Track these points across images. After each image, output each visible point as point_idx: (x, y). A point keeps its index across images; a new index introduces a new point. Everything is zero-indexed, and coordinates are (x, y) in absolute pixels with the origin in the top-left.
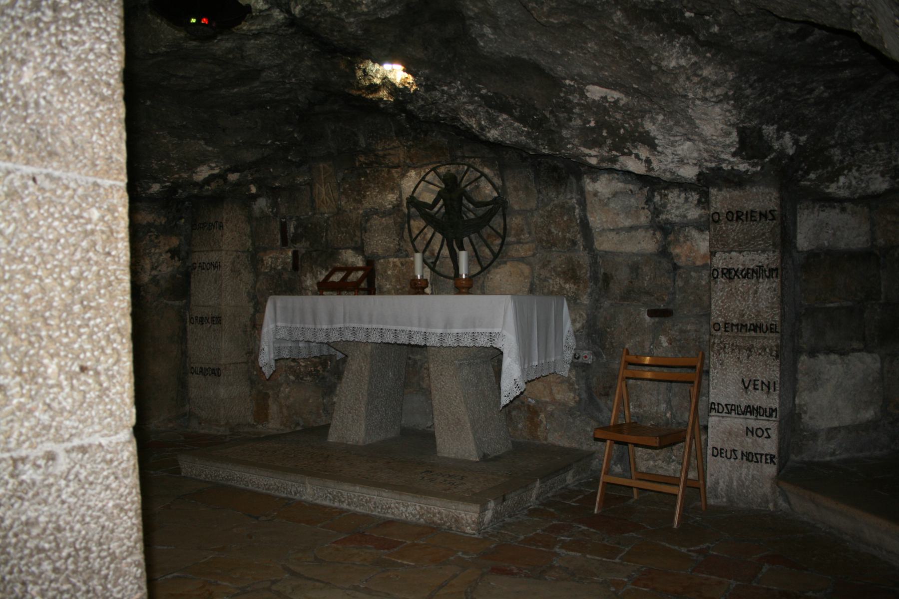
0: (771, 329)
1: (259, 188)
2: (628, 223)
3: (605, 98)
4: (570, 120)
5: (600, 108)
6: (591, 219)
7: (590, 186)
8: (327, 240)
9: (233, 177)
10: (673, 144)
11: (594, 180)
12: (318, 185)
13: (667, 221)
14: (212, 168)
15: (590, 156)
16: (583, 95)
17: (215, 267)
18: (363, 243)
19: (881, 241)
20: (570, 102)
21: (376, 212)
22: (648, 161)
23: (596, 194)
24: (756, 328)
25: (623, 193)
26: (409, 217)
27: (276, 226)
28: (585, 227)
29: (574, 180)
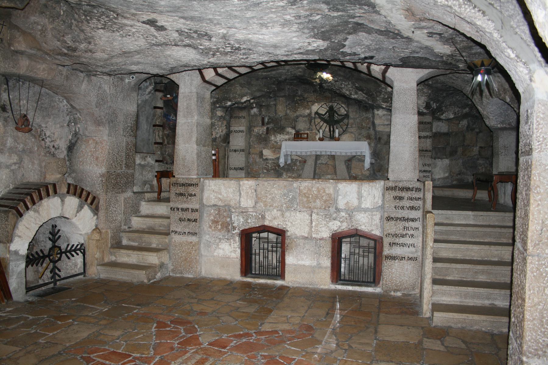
0: (430, 151)
1: (256, 105)
6: (375, 121)
7: (376, 112)
8: (281, 125)
9: (252, 101)
11: (378, 111)
14: (248, 98)
16: (386, 89)
17: (241, 132)
18: (295, 126)
19: (451, 130)
20: (382, 91)
21: (301, 116)
23: (378, 114)
24: (426, 151)
25: (387, 115)
26: (315, 118)
27: (259, 119)
28: (373, 123)
29: (371, 110)
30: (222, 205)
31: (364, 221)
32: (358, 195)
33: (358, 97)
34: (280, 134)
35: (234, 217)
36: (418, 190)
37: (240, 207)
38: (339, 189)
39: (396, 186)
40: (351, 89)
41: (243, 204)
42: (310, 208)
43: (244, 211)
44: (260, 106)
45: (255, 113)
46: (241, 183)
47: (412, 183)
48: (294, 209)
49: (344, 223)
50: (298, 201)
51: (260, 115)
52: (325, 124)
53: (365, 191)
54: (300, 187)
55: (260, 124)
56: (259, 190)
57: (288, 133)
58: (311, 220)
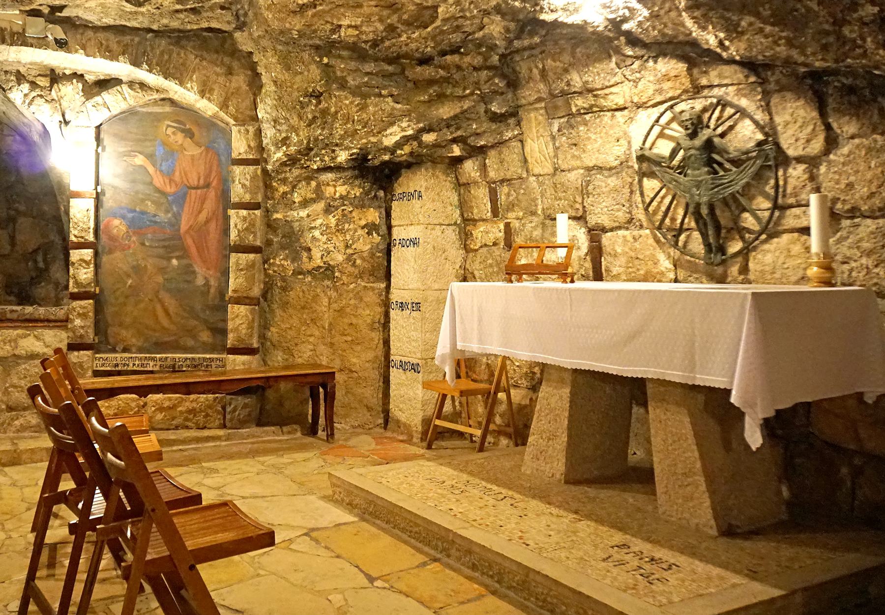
9: (429, 138)
12: (529, 140)
18: (585, 212)
33: (750, 48)
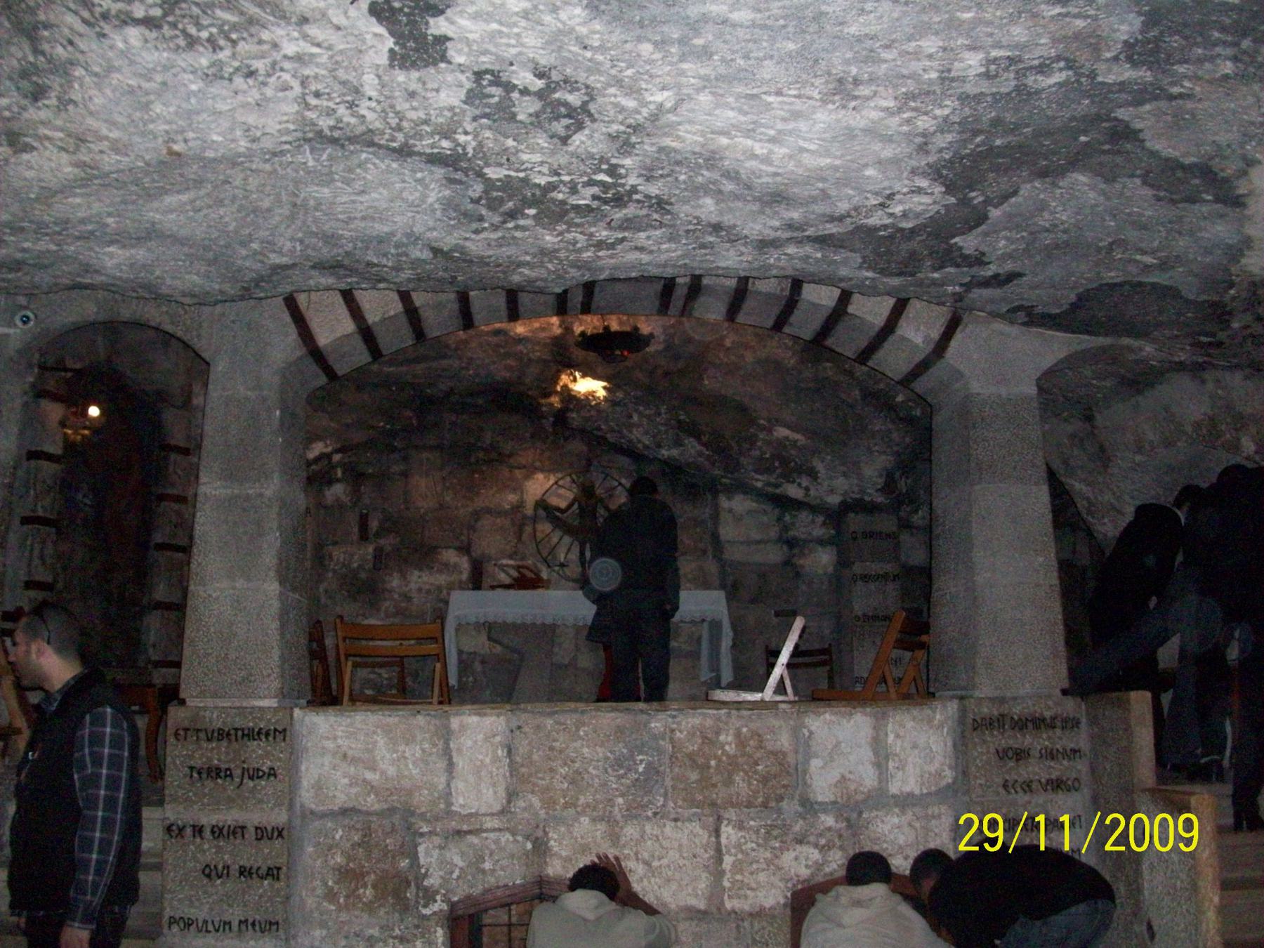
2: (758, 537)
3: (787, 438)
4: (750, 450)
5: (782, 443)
7: (724, 502)
10: (831, 478)
13: (795, 538)
14: (326, 446)
15: (757, 480)
18: (469, 545)
20: (756, 436)
21: (489, 511)
22: (807, 489)
23: (730, 511)
26: (535, 519)
27: (353, 519)
28: (715, 537)
29: (709, 497)
30: (377, 807)
31: (901, 840)
32: (876, 753)
33: (681, 455)
34: (421, 570)
35: (427, 853)
36: (1070, 725)
37: (449, 813)
38: (811, 733)
39: (1002, 716)
40: (663, 428)
41: (461, 801)
42: (713, 804)
43: (465, 827)
44: (356, 477)
45: (338, 500)
46: (455, 723)
47: (1050, 703)
48: (655, 814)
49: (831, 853)
50: (668, 782)
51: (355, 504)
52: (567, 540)
53: (897, 736)
54: (673, 731)
55: (355, 537)
56: (522, 748)
57: (446, 566)
58: (718, 850)
